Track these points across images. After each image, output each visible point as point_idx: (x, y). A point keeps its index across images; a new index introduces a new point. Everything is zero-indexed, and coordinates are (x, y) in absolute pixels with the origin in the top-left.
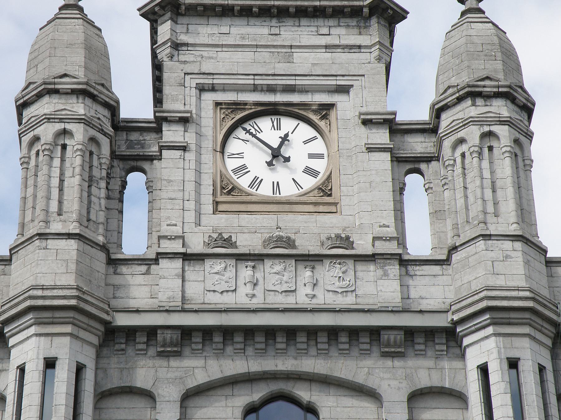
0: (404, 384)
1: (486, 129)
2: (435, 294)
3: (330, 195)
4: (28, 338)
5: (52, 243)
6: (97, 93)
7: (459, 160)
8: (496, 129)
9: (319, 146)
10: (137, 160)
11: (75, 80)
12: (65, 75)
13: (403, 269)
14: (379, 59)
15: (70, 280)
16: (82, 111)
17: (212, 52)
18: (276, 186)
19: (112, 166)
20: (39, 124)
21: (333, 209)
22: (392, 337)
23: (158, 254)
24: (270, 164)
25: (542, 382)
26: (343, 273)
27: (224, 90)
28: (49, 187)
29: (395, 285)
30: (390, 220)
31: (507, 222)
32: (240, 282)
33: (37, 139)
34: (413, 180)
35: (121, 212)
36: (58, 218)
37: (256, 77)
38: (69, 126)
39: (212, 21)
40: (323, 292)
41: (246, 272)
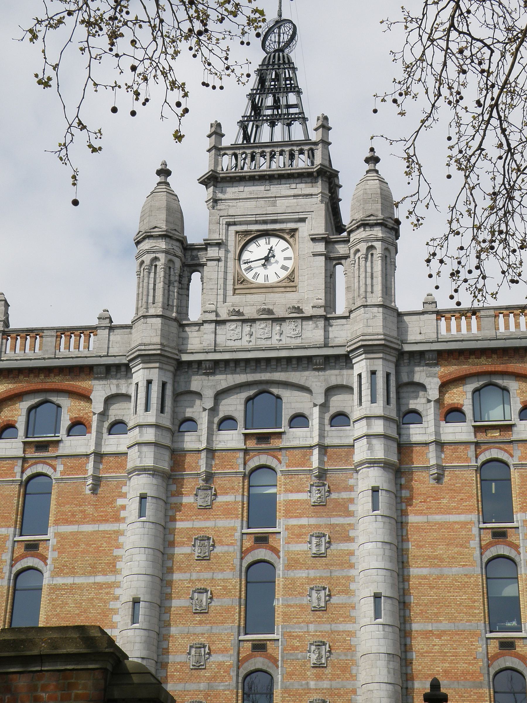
0: (324, 384)
1: (370, 244)
2: (342, 335)
3: (293, 281)
4: (139, 369)
5: (149, 320)
8: (375, 244)
9: (289, 253)
10: (196, 266)
11: (160, 230)
12: (156, 227)
13: (327, 322)
15: (157, 340)
16: (164, 247)
17: (234, 203)
18: (267, 277)
19: (184, 271)
20: (143, 254)
21: (294, 289)
23: (203, 321)
26: (296, 327)
28: (148, 289)
29: (321, 332)
31: (377, 298)
32: (244, 334)
33: (142, 262)
35: (188, 296)
36: (153, 306)
37: (257, 216)
38: (158, 255)
39: (235, 184)
41: (247, 328)
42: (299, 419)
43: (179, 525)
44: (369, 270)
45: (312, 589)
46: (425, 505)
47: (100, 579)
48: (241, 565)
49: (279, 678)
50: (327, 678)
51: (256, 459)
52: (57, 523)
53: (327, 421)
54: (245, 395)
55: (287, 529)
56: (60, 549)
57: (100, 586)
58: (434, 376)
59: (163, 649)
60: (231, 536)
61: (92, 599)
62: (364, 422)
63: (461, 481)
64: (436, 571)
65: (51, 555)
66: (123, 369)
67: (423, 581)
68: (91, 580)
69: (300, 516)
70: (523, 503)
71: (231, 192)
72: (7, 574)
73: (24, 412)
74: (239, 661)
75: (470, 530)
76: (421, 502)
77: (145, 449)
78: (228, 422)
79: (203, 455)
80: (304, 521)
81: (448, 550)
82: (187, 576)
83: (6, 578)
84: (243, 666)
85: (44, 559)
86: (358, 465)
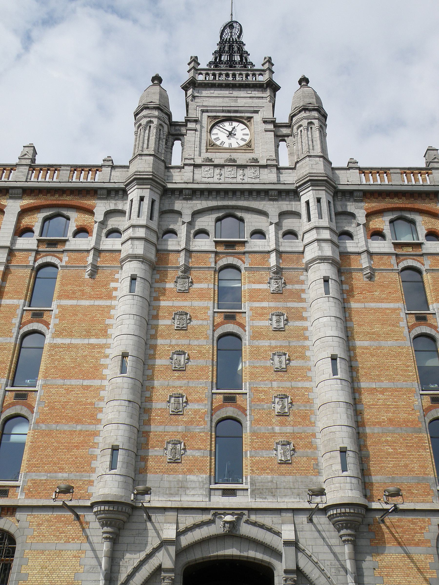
1: (310, 121)
2: (290, 179)
3: (251, 147)
5: (143, 157)
6: (163, 108)
7: (299, 133)
9: (247, 131)
14: (270, 102)
15: (151, 170)
17: (207, 99)
22: (273, 193)
24: (228, 137)
25: (329, 207)
27: (211, 112)
28: (144, 139)
29: (275, 175)
30: (274, 155)
32: (215, 174)
33: (140, 125)
34: (282, 144)
38: (152, 119)
40: (248, 178)
41: (217, 171)
42: (259, 233)
43: (163, 303)
44: (310, 136)
45: (274, 354)
47: (93, 341)
48: (213, 336)
49: (247, 424)
50: (290, 424)
51: (224, 259)
52: (60, 297)
53: (280, 235)
54: (215, 216)
55: (251, 310)
56: (61, 317)
57: (93, 346)
58: (361, 208)
59: (146, 397)
60: (204, 313)
61: (86, 356)
62: (314, 231)
63: (388, 280)
65: (53, 322)
66: (121, 193)
67: (365, 351)
68: (86, 341)
69: (262, 300)
70: (437, 296)
71: (205, 93)
72: (15, 334)
73: (40, 220)
74: (212, 409)
76: (358, 293)
77: (136, 242)
78: (203, 232)
79: (183, 254)
80: (265, 304)
81: (383, 328)
82: (168, 341)
83: (14, 336)
84: (216, 414)
85: (47, 324)
86: (310, 262)
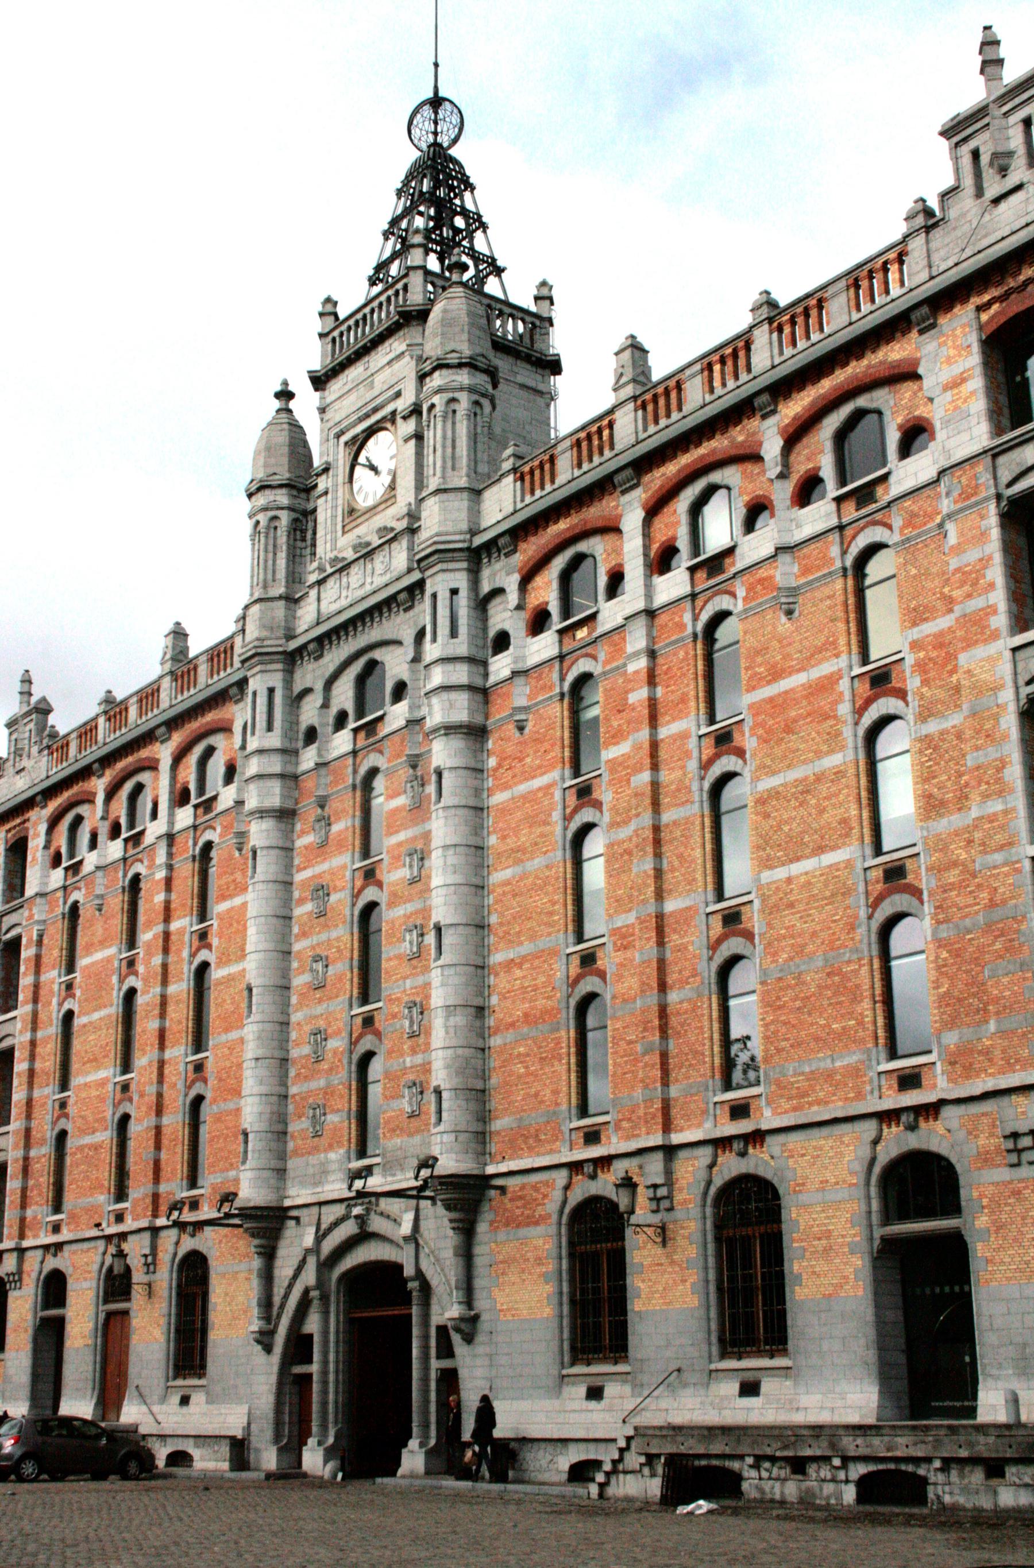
46: (509, 772)
64: (518, 870)
75: (552, 794)
80: (402, 836)
